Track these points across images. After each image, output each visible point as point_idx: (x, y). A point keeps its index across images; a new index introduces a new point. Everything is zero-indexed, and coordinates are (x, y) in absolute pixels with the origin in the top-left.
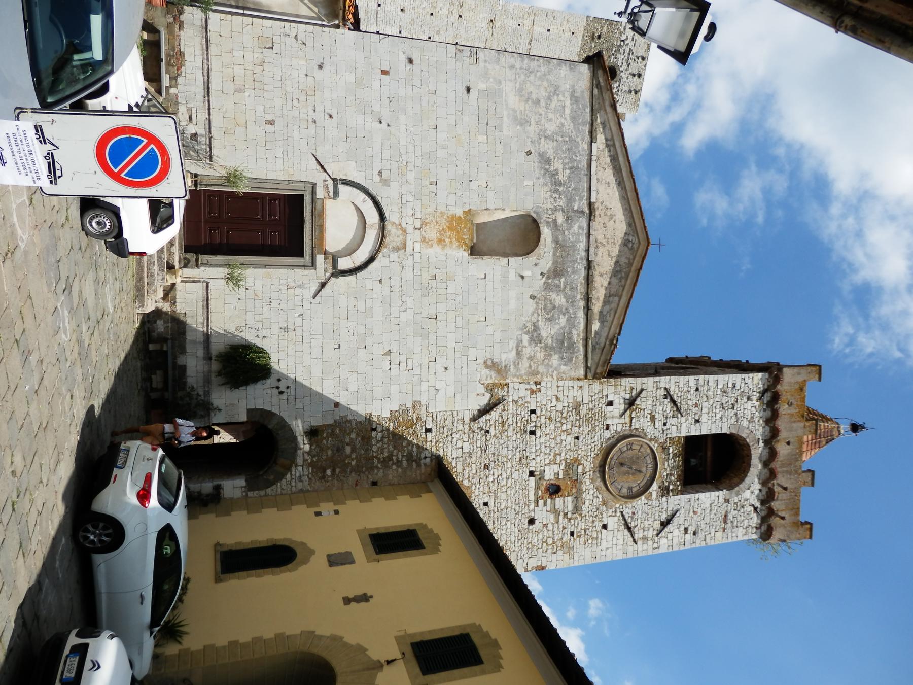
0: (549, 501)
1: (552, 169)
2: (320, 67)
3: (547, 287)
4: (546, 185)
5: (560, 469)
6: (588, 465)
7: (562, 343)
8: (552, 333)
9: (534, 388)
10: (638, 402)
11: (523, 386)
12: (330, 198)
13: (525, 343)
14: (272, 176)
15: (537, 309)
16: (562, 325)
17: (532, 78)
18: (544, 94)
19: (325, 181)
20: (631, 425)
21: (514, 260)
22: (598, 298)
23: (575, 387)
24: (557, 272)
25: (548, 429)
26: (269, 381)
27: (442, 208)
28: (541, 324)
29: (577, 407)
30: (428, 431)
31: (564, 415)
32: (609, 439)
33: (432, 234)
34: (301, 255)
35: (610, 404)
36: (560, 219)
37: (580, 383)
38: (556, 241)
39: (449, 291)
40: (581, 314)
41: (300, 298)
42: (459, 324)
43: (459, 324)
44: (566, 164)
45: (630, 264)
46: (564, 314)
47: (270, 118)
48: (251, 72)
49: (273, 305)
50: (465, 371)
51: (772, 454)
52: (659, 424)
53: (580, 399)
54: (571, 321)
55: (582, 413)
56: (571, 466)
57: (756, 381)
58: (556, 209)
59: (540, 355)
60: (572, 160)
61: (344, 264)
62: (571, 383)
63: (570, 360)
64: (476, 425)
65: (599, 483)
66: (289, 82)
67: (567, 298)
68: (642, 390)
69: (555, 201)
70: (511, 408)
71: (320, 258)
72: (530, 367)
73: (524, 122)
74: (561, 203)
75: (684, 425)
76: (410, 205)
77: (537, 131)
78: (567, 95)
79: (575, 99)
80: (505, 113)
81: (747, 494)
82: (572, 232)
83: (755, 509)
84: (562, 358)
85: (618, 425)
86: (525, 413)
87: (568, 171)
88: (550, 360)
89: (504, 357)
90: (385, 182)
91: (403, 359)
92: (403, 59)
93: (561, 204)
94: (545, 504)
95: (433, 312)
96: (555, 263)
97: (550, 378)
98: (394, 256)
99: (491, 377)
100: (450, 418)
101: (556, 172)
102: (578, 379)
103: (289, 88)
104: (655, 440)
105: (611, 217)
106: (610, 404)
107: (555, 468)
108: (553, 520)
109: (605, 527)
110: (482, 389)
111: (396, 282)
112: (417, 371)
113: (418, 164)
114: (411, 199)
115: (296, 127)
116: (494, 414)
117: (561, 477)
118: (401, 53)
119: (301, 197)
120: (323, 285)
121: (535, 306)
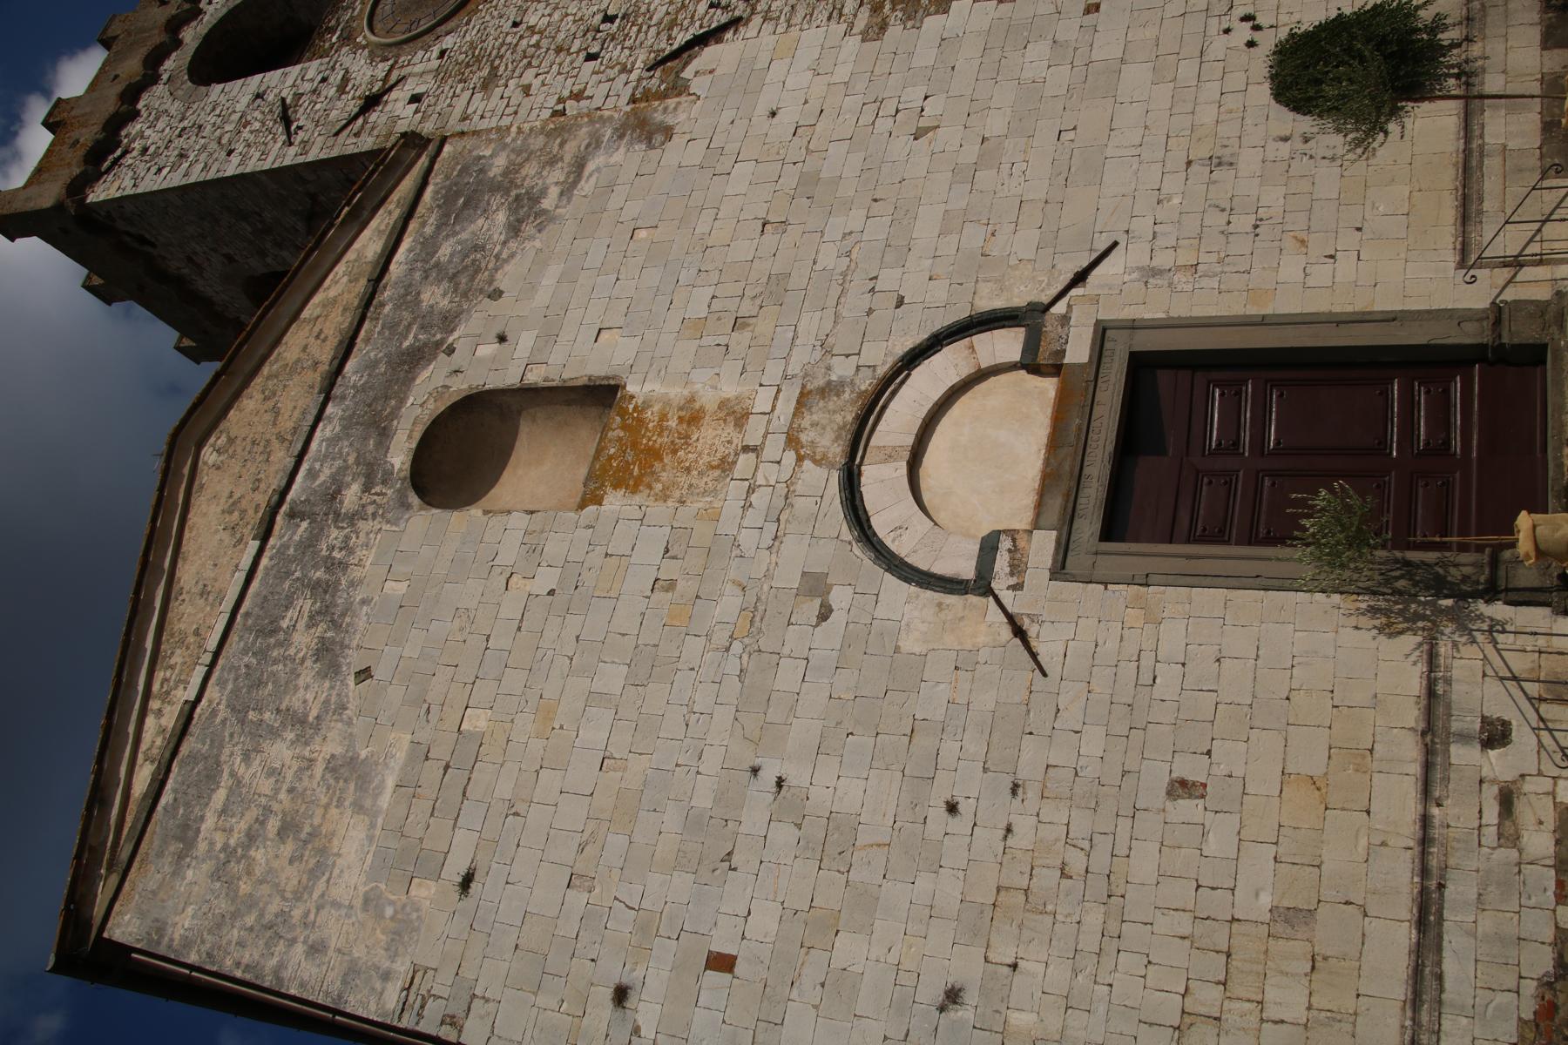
1: (322, 627)
2: (953, 996)
3: (449, 321)
4: (352, 584)
7: (465, 204)
8: (480, 222)
9: (571, 106)
10: (356, 110)
11: (597, 102)
12: (1012, 534)
13: (554, 192)
14: (1208, 598)
15: (497, 270)
16: (452, 240)
17: (273, 908)
18: (258, 854)
19: (1018, 587)
20: (392, 67)
21: (509, 377)
22: (345, 310)
23: (476, 118)
24: (415, 358)
25: (573, 29)
26: (1283, 34)
27: (658, 510)
29: (487, 85)
31: (525, 61)
32: (448, 33)
33: (712, 438)
34: (1142, 366)
35: (416, 99)
38: (385, 434)
39: (710, 291)
40: (396, 268)
41: (1159, 242)
42: (708, 215)
43: (708, 215)
44: (280, 644)
46: (437, 265)
47: (1187, 808)
48: (1237, 989)
49: (1252, 219)
50: (727, 115)
51: (154, 60)
53: (478, 96)
54: (428, 246)
55: (485, 73)
57: (116, 185)
58: (353, 518)
60: (262, 654)
61: (1006, 345)
62: (484, 124)
63: (465, 170)
64: (737, 13)
66: (1090, 942)
67: (417, 301)
68: (337, 134)
69: (347, 538)
70: (642, 58)
71: (1078, 352)
72: (562, 145)
74: (335, 535)
75: (289, 82)
76: (753, 518)
77: (318, 739)
78: (202, 846)
79: (187, 834)
80: (385, 801)
82: (339, 463)
84: (482, 171)
87: (285, 624)
88: (512, 163)
89: (618, 157)
90: (815, 586)
91: (884, 125)
92: (646, 1011)
93: (334, 533)
95: (770, 238)
96: (408, 381)
97: (526, 127)
98: (842, 369)
100: (797, 19)
102: (463, 133)
103: (1094, 919)
111: (856, 301)
112: (851, 102)
113: (694, 646)
114: (747, 539)
115: (1088, 773)
118: (648, 1032)
119: (1110, 532)
120: (1080, 278)
121: (499, 275)
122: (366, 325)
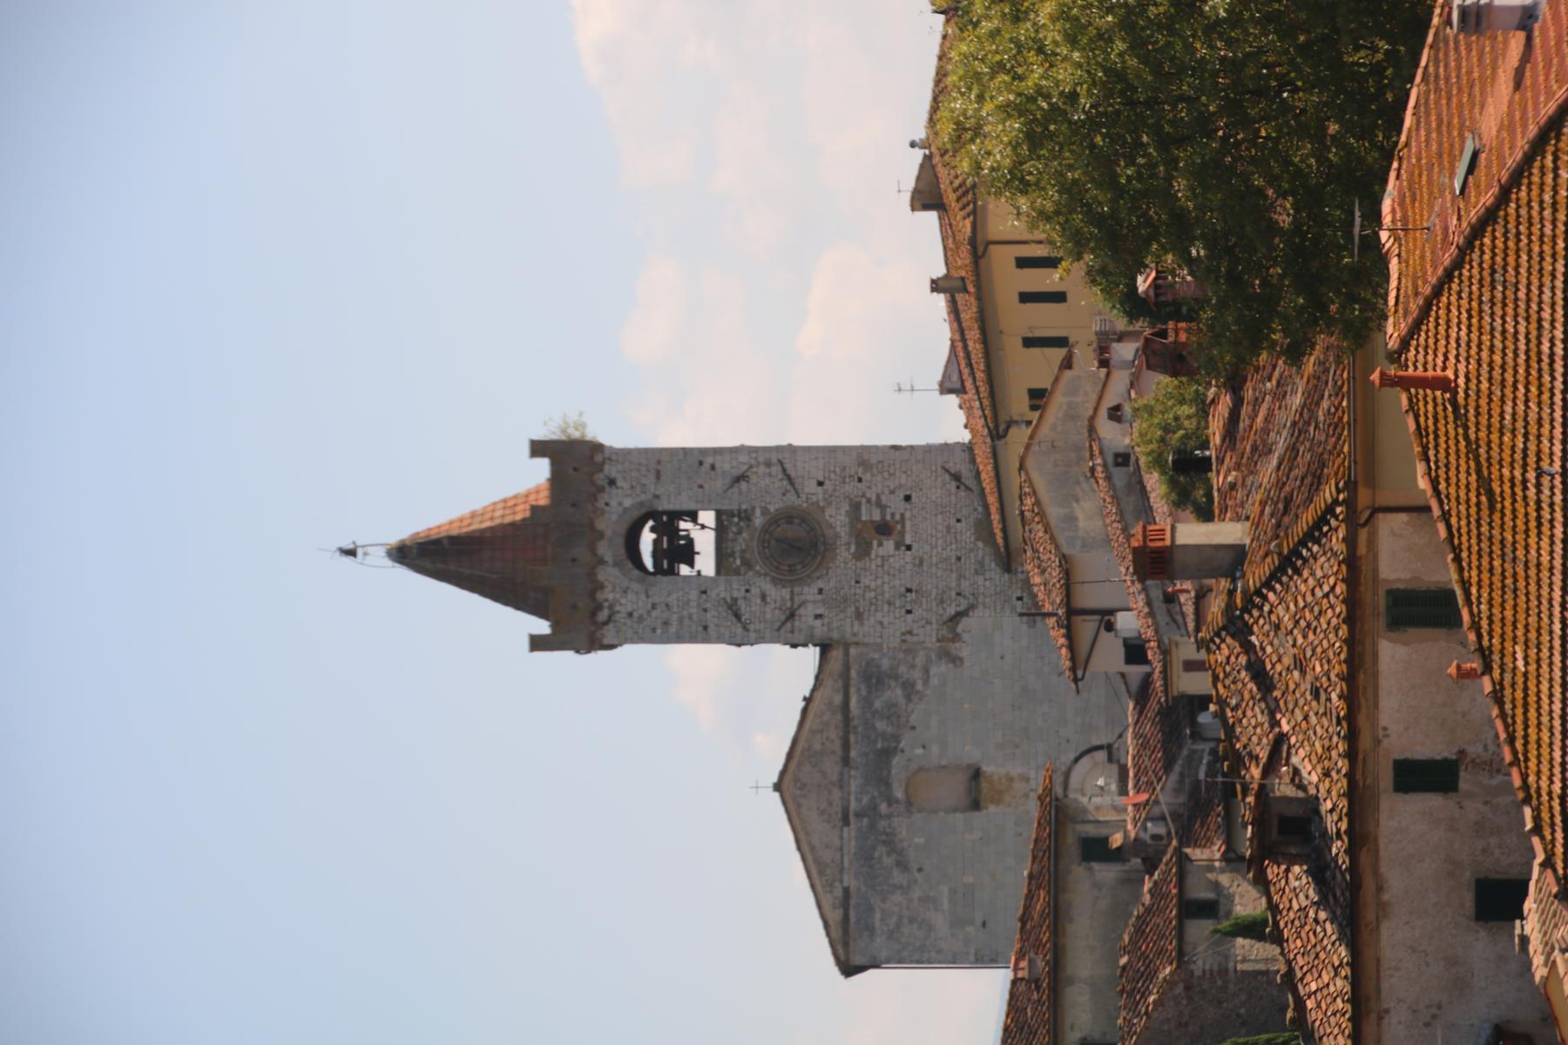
0: (888, 518)
3: (896, 738)
5: (876, 550)
6: (844, 554)
9: (908, 637)
10: (783, 617)
11: (921, 638)
17: (918, 944)
24: (887, 754)
28: (902, 701)
30: (1020, 599)
33: (1019, 786)
35: (818, 617)
36: (883, 808)
37: (854, 639)
38: (888, 785)
45: (799, 764)
52: (755, 591)
56: (863, 551)
58: (889, 817)
59: (902, 669)
61: (1101, 756)
62: (867, 640)
63: (868, 664)
65: (829, 533)
67: (874, 727)
73: (926, 900)
74: (882, 824)
79: (871, 930)
81: (627, 503)
83: (612, 482)
84: (878, 666)
85: (810, 592)
86: (918, 612)
89: (943, 668)
94: (893, 515)
99: (954, 648)
101: (888, 854)
102: (857, 644)
104: (759, 574)
105: (823, 812)
106: (818, 617)
107: (881, 552)
108: (883, 498)
109: (820, 484)
110: (965, 636)
116: (952, 611)
117: (875, 543)
122: (852, 738)
